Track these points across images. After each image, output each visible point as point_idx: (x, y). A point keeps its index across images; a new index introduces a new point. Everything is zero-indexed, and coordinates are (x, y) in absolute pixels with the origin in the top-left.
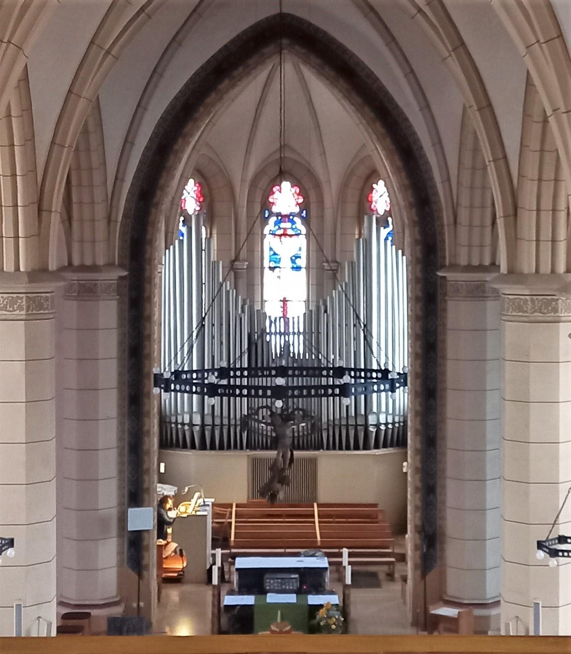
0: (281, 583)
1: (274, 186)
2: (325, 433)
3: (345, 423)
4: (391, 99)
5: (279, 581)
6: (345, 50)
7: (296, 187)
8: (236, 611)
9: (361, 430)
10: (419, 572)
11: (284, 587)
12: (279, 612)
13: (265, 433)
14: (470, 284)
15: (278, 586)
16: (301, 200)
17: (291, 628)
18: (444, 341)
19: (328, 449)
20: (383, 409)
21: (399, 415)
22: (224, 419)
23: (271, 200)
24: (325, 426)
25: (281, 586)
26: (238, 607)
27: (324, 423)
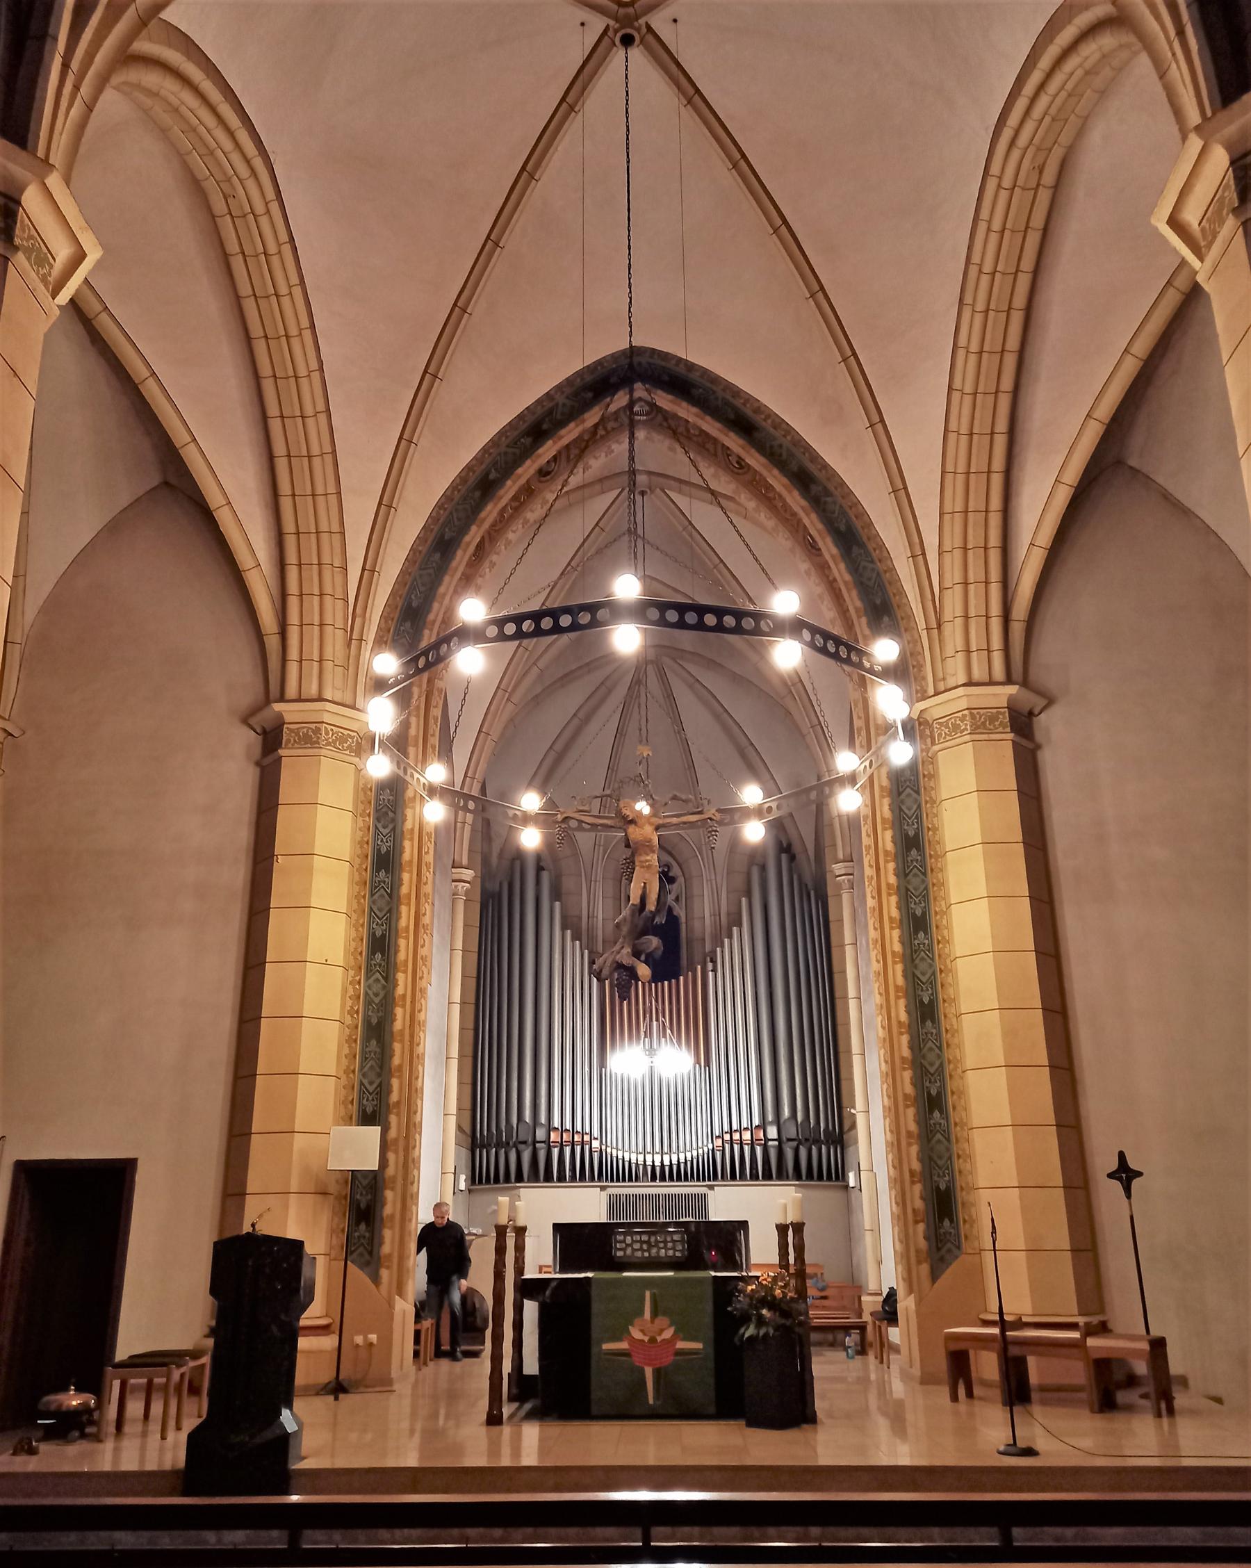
0: (648, 1242)
4: (815, 457)
5: (645, 1238)
6: (737, 392)
8: (548, 1293)
9: (773, 1146)
10: (925, 1268)
11: (654, 1251)
12: (648, 1294)
14: (978, 713)
15: (641, 1249)
17: (675, 1331)
18: (935, 829)
25: (648, 1250)
26: (554, 1284)
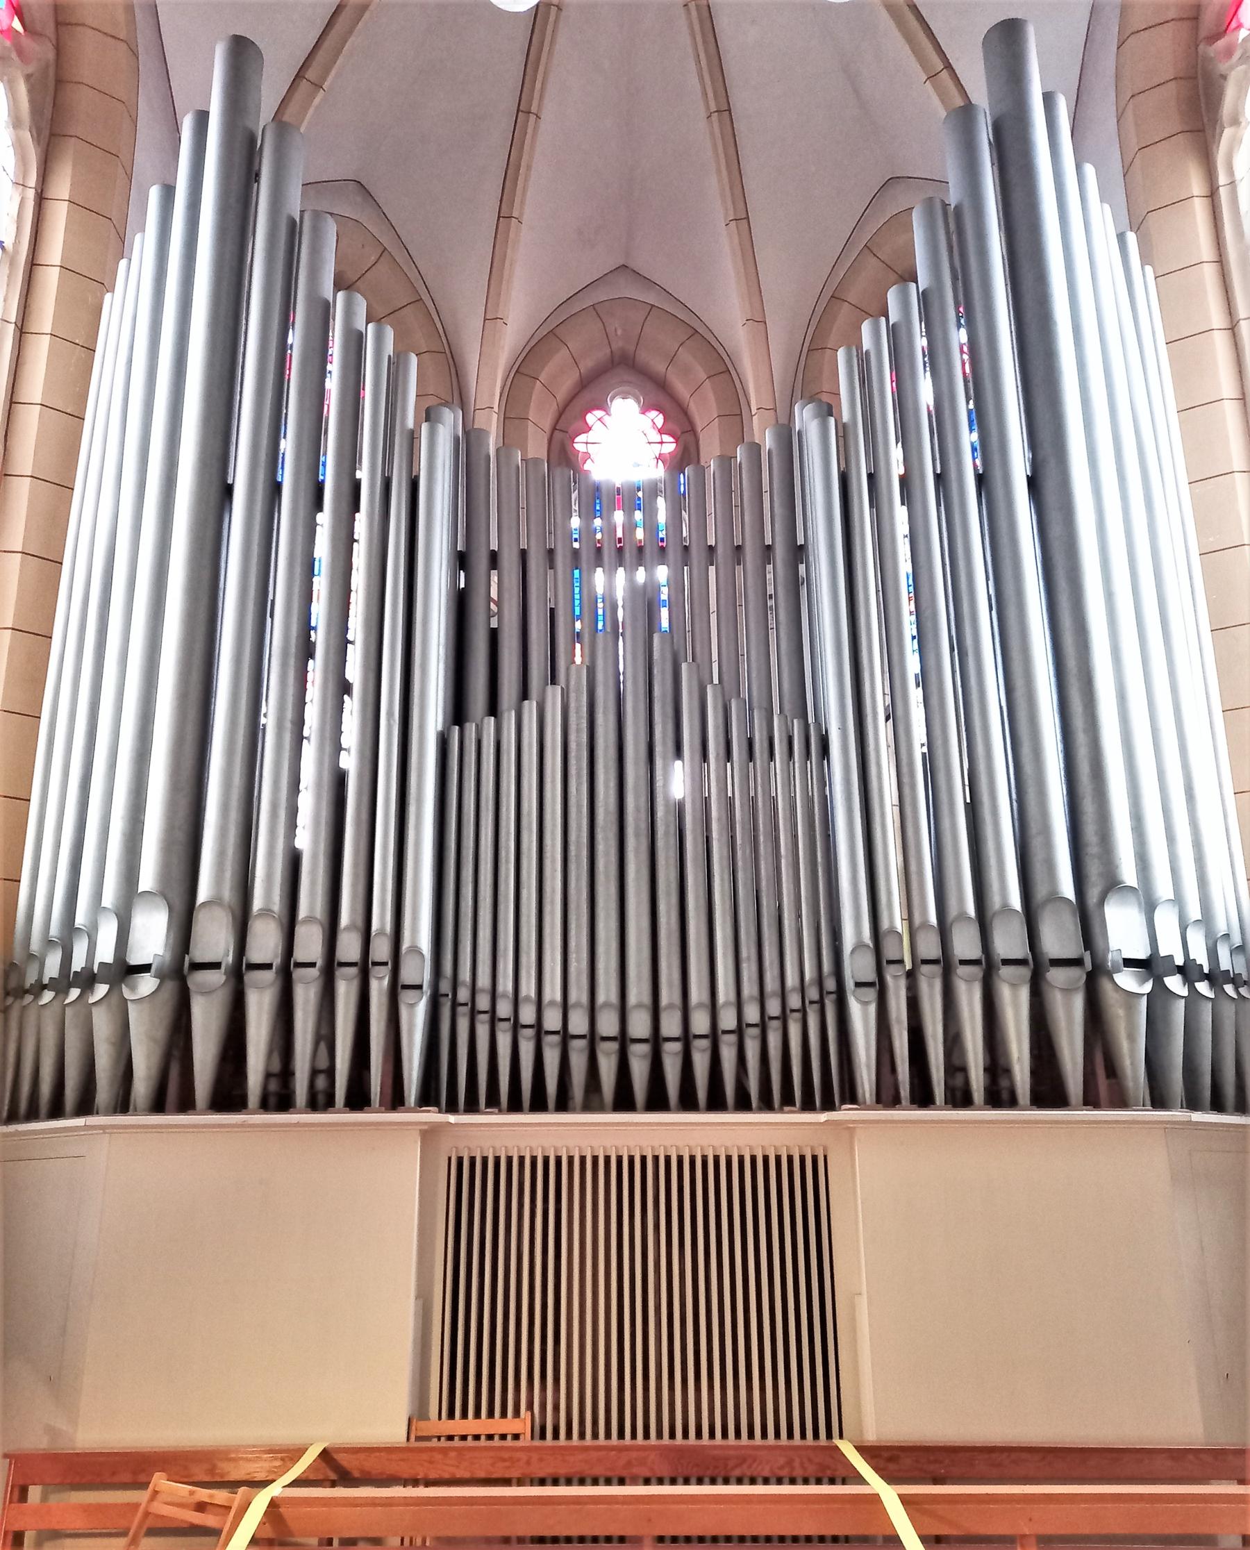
1: (590, 410)
2: (865, 1004)
3: (975, 952)
7: (653, 414)
13: (527, 1015)
16: (669, 447)
19: (887, 1097)
20: (1163, 888)
21: (1227, 936)
22: (300, 931)
23: (579, 447)
24: (858, 966)
27: (859, 946)
